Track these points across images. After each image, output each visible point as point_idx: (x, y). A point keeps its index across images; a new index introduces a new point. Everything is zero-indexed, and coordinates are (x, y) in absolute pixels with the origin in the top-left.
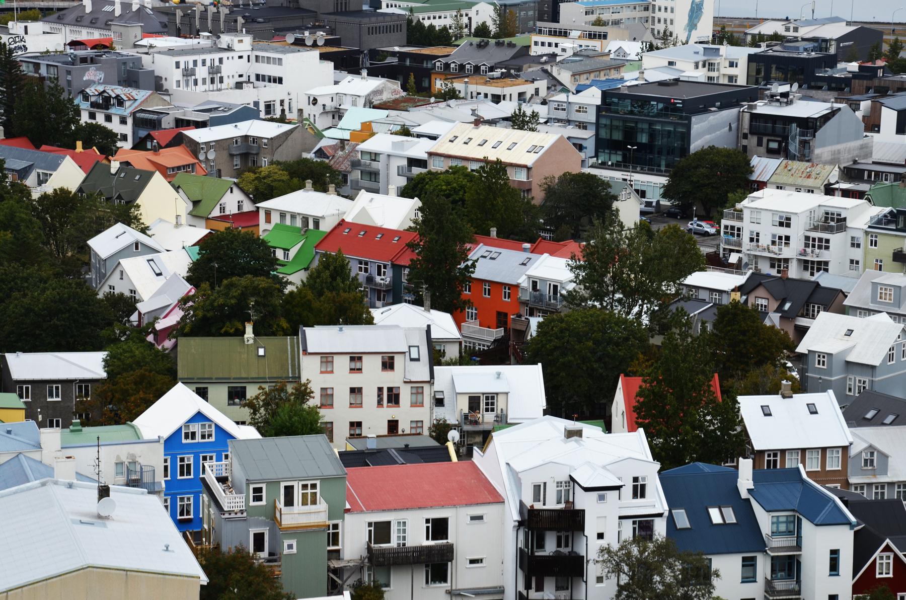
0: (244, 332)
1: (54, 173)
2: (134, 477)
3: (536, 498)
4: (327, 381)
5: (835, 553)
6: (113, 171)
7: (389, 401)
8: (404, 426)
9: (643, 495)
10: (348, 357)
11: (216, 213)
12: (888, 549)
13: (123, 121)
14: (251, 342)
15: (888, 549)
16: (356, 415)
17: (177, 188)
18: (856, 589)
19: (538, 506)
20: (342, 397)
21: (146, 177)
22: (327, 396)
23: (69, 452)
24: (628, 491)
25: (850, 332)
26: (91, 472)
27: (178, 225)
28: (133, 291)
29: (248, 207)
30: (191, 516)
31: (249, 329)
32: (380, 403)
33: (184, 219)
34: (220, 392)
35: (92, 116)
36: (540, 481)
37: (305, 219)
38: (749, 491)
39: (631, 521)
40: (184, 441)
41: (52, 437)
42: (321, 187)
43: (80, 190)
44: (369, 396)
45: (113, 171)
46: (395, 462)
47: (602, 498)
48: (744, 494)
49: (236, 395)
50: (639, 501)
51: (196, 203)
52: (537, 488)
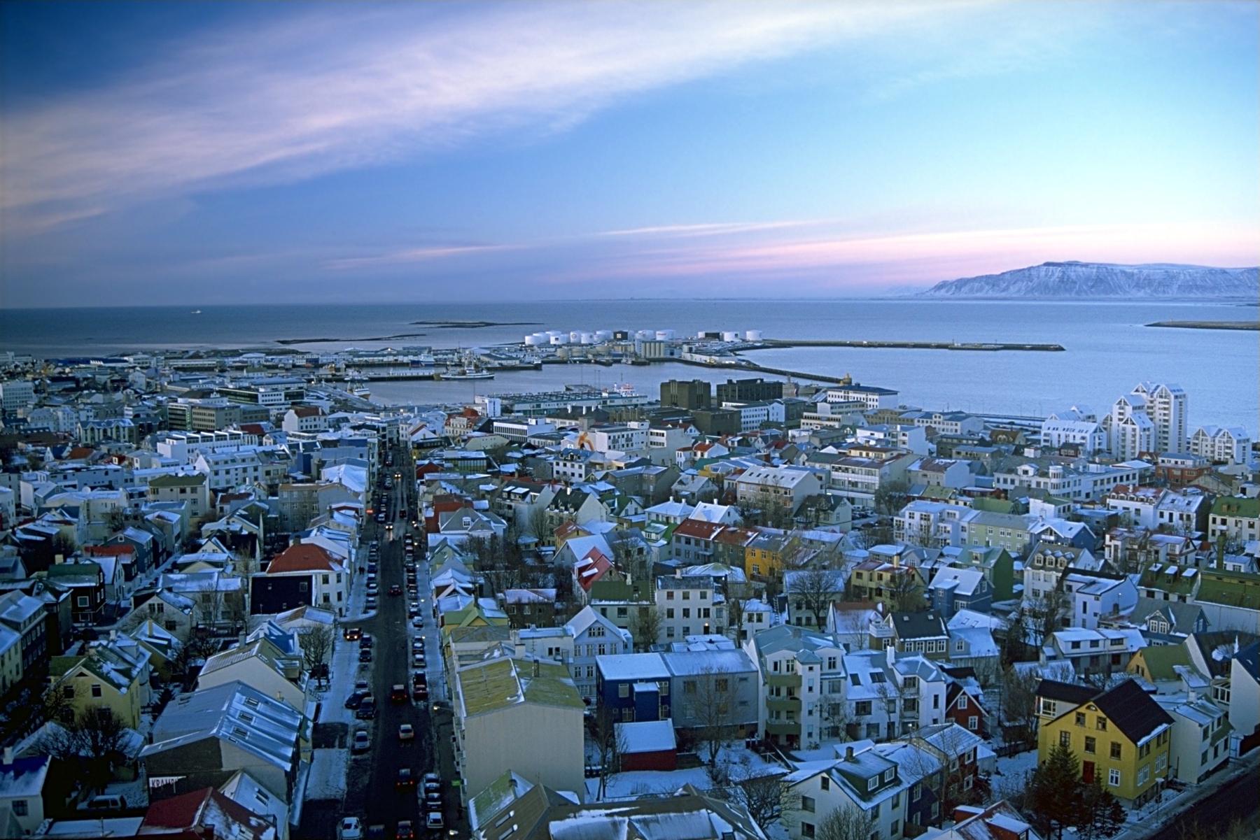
3: (776, 669)
5: (936, 697)
7: (705, 616)
9: (834, 667)
20: (678, 613)
22: (670, 614)
24: (826, 664)
25: (956, 578)
32: (699, 616)
36: (777, 660)
38: (893, 664)
42: (678, 500)
47: (811, 669)
48: (890, 666)
50: (832, 671)
52: (776, 664)
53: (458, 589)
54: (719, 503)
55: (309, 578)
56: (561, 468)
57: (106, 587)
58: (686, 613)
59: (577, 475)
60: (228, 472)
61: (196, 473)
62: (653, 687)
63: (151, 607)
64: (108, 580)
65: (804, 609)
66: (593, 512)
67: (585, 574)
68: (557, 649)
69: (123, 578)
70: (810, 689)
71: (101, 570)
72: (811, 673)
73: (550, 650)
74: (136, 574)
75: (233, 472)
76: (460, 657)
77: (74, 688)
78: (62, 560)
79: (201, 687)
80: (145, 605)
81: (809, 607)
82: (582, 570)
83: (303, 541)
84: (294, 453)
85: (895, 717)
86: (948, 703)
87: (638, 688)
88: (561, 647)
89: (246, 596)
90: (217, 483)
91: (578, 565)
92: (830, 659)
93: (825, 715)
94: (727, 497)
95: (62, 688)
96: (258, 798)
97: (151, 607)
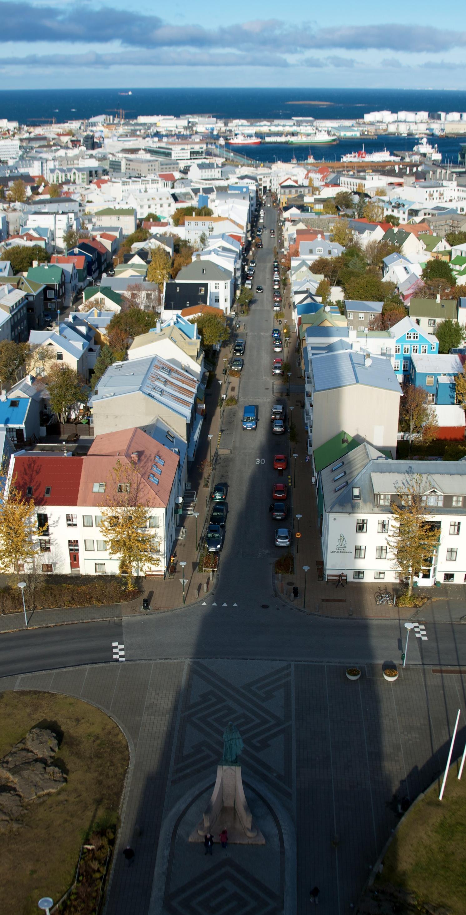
2: (383, 352)
6: (395, 232)
13: (404, 213)
21: (408, 234)
23: (359, 339)
26: (364, 347)
28: (398, 279)
30: (399, 369)
31: (439, 296)
33: (422, 251)
35: (393, 211)
40: (407, 339)
43: (383, 239)
45: (395, 232)
55: (206, 286)
56: (389, 213)
57: (66, 285)
60: (150, 207)
63: (96, 300)
64: (68, 279)
69: (77, 279)
74: (86, 277)
75: (153, 206)
76: (313, 348)
79: (130, 357)
84: (196, 194)
90: (142, 214)
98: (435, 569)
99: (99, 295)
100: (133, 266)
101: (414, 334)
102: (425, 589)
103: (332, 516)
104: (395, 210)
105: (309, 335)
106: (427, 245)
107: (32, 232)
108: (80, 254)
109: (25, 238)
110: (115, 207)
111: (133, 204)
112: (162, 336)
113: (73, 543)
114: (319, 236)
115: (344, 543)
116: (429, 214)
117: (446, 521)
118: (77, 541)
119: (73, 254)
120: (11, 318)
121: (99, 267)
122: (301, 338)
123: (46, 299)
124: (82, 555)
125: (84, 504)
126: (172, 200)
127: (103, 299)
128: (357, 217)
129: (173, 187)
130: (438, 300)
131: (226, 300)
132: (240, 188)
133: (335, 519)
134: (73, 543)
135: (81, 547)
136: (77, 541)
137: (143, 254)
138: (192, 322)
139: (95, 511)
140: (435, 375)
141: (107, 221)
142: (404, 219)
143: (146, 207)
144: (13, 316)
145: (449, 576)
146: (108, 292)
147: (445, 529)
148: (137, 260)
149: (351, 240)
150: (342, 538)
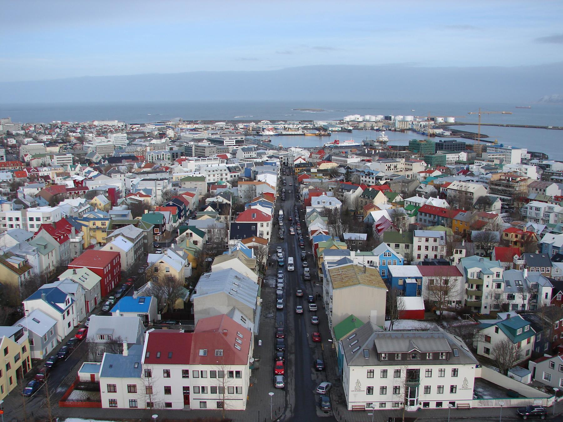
0: (399, 230)
1: (356, 191)
4: (420, 244)
6: (370, 190)
8: (438, 257)
10: (425, 239)
11: (394, 201)
12: (560, 293)
13: (373, 178)
14: (401, 233)
15: (560, 293)
16: (427, 253)
17: (385, 195)
18: (551, 303)
19: (472, 278)
20: (423, 248)
22: (419, 248)
24: (495, 275)
25: (554, 238)
27: (384, 204)
28: (373, 220)
29: (402, 200)
32: (433, 250)
33: (386, 202)
34: (393, 245)
35: (366, 177)
37: (416, 204)
39: (495, 283)
41: (353, 253)
42: (420, 195)
43: (362, 195)
44: (430, 249)
45: (370, 190)
46: (435, 265)
49: (397, 246)
50: (498, 278)
51: (389, 199)
52: (472, 273)
53: (322, 232)
54: (440, 198)
58: (427, 248)
59: (371, 182)
60: (214, 176)
61: (200, 176)
62: (414, 281)
63: (187, 234)
64: (167, 222)
65: (480, 249)
66: (380, 199)
67: (379, 228)
68: (371, 261)
69: (172, 221)
70: (487, 286)
71: (164, 217)
72: (488, 278)
73: (368, 262)
74: (178, 220)
75: (216, 175)
76: (328, 263)
77: (159, 268)
78: (147, 213)
79: (213, 270)
80: (185, 234)
81: (483, 248)
82: (378, 226)
83: (252, 207)
85: (526, 302)
86: (552, 297)
87: (408, 281)
88: (373, 260)
89: (228, 231)
90: (209, 180)
91: (376, 224)
92: (497, 273)
93: (493, 298)
94: (443, 196)
95: (154, 268)
96: (241, 319)
97: (187, 234)
98: (417, 400)
99: (189, 231)
100: (208, 213)
101: (389, 253)
102: (412, 413)
103: (351, 368)
104: (368, 177)
105: (325, 255)
106: (389, 199)
107: (142, 192)
108: (174, 205)
109: (138, 196)
110: (193, 176)
111: (204, 174)
112: (233, 257)
113: (186, 389)
114: (324, 193)
115: (360, 385)
116: (388, 180)
117: (423, 369)
118: (189, 387)
119: (168, 205)
120: (134, 246)
121: (185, 214)
122: (318, 257)
123: (154, 234)
124: (192, 396)
125: (194, 363)
126: (227, 171)
127: (191, 234)
128: (345, 181)
129: (227, 164)
130: (401, 232)
131: (268, 234)
132: (271, 164)
133: (353, 370)
134: (186, 389)
135: (191, 391)
136: (189, 387)
137: (213, 205)
138: (250, 247)
139: (200, 368)
140: (404, 279)
141: (188, 185)
142: (373, 182)
143: (212, 176)
144: (135, 244)
145: (426, 404)
146: (194, 229)
147: (422, 374)
148: (210, 209)
149: (342, 196)
150: (358, 382)
